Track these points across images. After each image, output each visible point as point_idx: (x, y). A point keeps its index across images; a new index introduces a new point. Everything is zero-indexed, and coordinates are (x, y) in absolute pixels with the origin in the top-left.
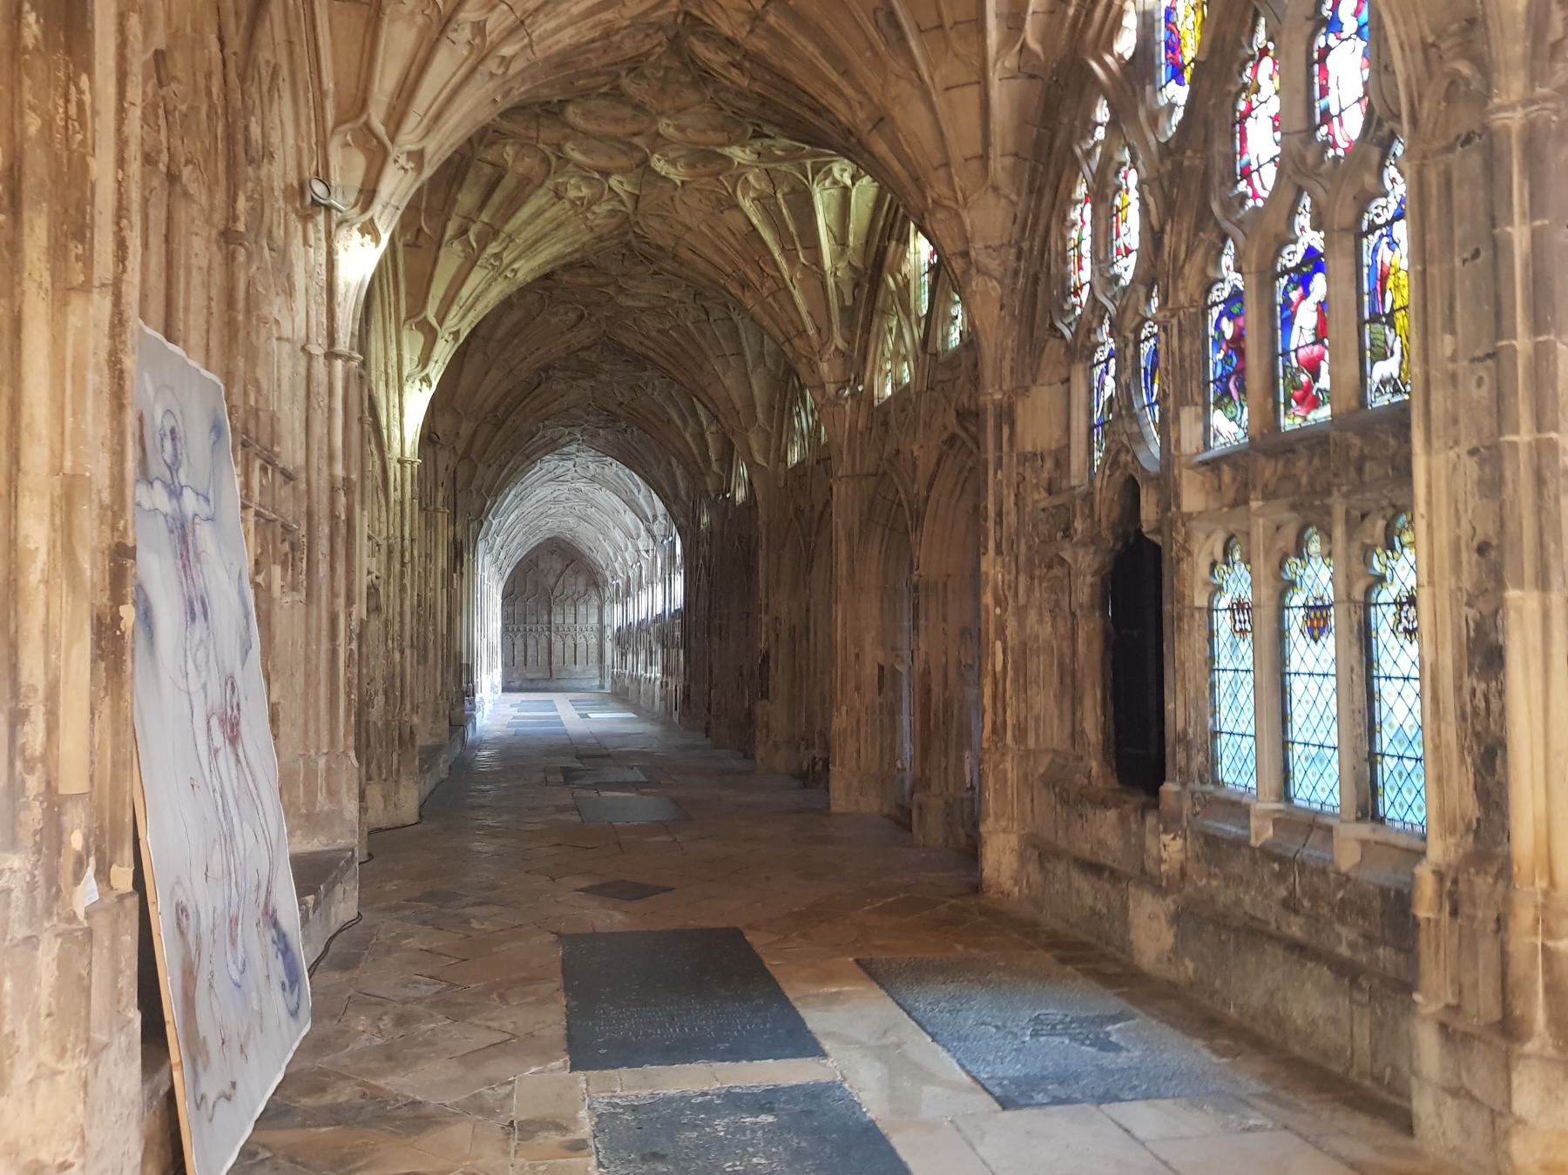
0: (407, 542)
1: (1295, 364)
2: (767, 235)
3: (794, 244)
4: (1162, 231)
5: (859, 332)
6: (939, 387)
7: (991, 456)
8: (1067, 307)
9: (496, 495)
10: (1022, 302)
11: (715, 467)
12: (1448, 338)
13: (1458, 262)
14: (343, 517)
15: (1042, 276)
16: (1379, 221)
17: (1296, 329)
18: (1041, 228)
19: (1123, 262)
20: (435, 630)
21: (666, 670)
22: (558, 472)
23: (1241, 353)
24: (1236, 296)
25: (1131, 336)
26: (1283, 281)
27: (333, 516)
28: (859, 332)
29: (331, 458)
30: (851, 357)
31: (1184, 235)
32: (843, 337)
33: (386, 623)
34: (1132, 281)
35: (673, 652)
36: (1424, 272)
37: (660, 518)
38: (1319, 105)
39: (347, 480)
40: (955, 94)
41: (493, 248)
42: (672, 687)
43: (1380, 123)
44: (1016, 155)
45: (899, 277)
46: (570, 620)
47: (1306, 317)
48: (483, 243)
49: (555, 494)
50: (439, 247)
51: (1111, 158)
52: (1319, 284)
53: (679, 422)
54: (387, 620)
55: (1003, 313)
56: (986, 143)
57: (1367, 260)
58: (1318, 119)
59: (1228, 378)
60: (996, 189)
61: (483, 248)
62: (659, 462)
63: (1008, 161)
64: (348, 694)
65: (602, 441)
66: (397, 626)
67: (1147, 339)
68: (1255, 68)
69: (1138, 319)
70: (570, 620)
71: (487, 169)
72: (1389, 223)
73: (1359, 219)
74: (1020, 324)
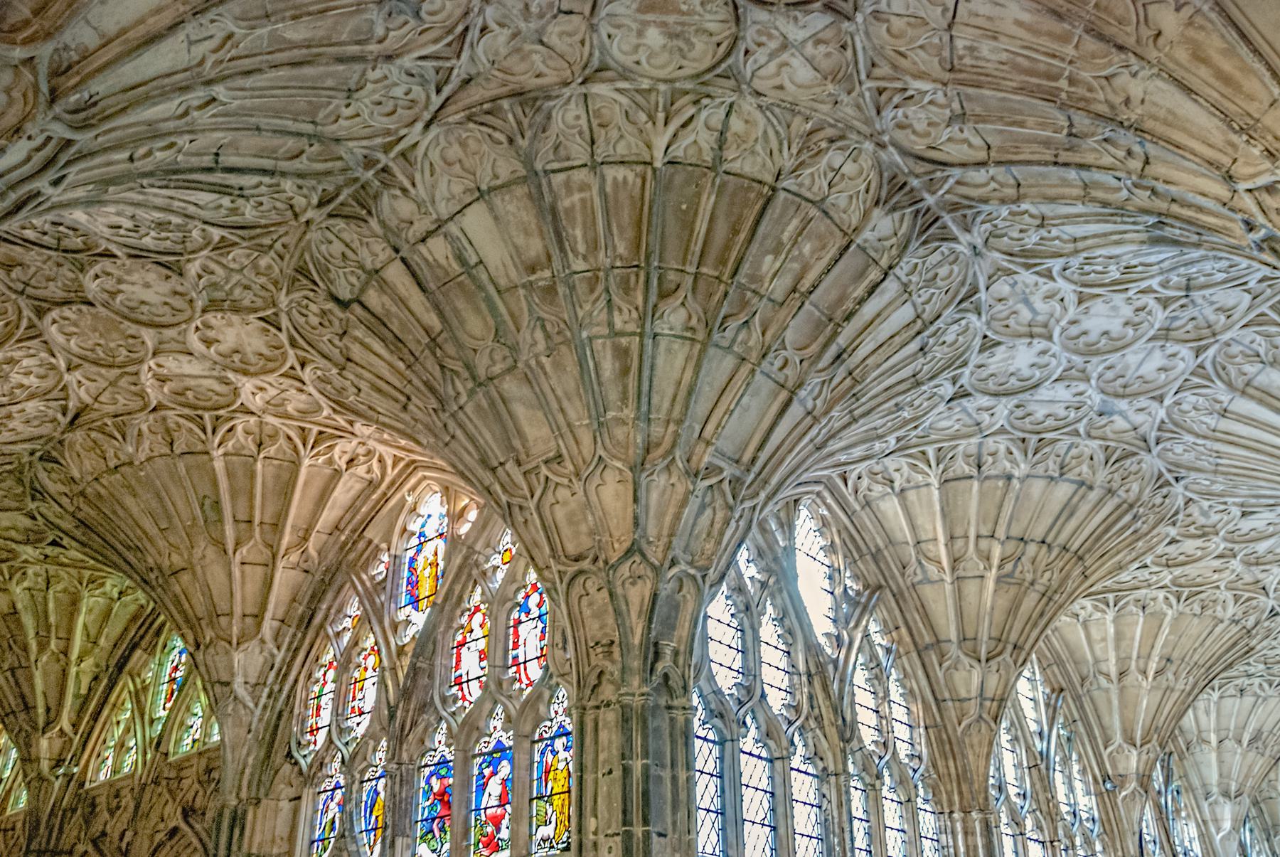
1: (483, 818)
2: (28, 621)
3: (49, 632)
4: (397, 706)
5: (86, 719)
6: (164, 783)
8: (303, 742)
10: (266, 730)
12: (593, 820)
13: (600, 775)
15: (286, 714)
16: (545, 736)
17: (486, 794)
18: (291, 678)
19: (358, 719)
23: (448, 805)
24: (443, 762)
25: (358, 776)
26: (479, 760)
28: (86, 719)
30: (71, 740)
31: (411, 713)
32: (70, 719)
34: (363, 736)
36: (581, 777)
38: (512, 653)
40: (246, 567)
43: (551, 676)
45: (138, 681)
47: (494, 787)
51: (356, 644)
52: (505, 769)
55: (250, 736)
56: (263, 606)
57: (537, 758)
58: (510, 662)
59: (433, 820)
60: (263, 641)
63: (276, 624)
67: (369, 780)
68: (471, 617)
69: (365, 764)
72: (552, 739)
73: (533, 732)
74: (261, 746)
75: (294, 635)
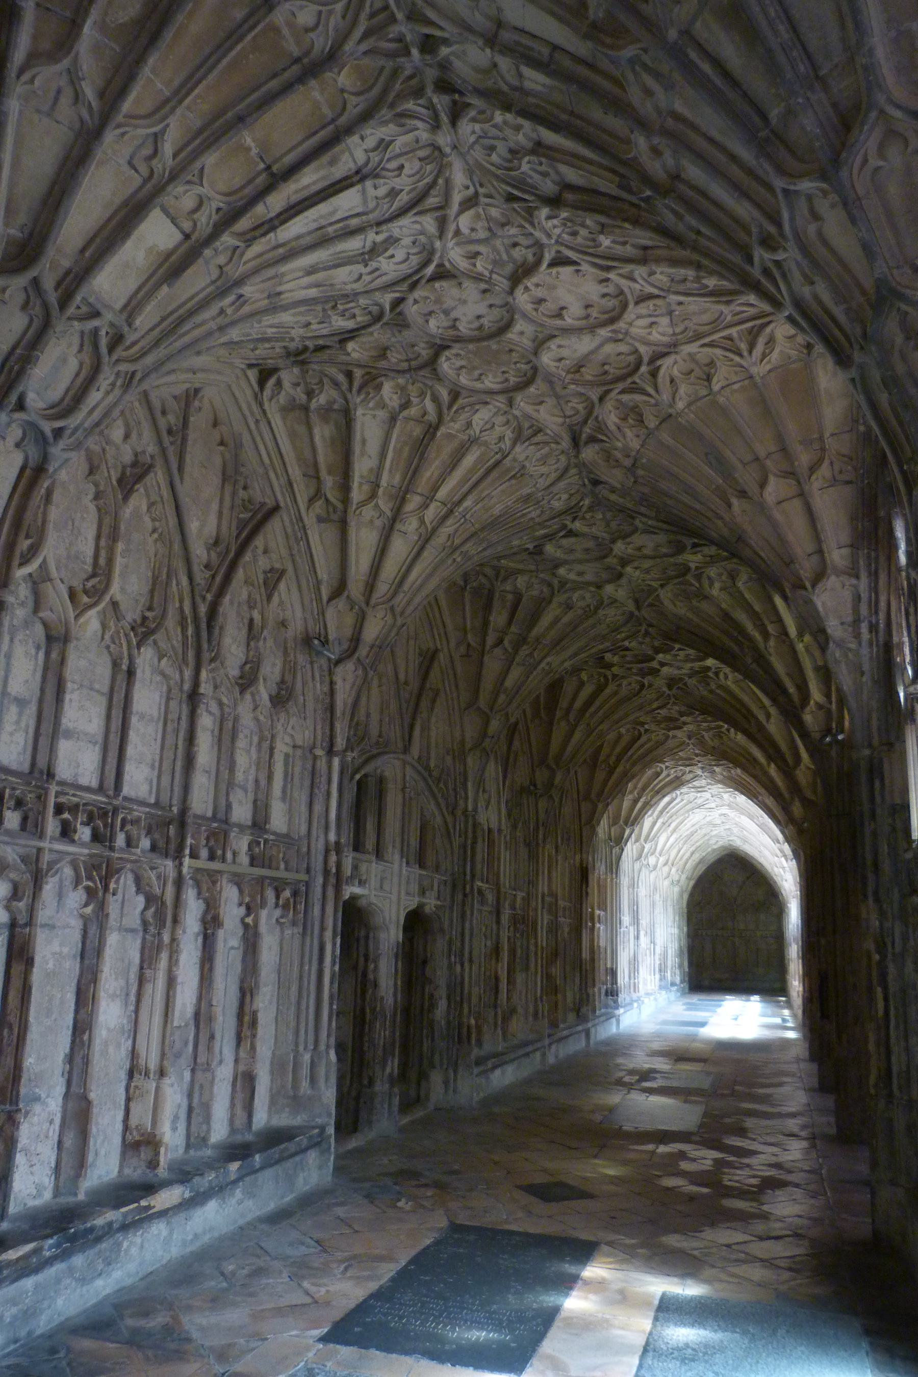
0: (468, 877)
2: (741, 616)
7: (866, 807)
9: (633, 825)
14: (334, 870)
20: (536, 943)
22: (699, 801)
27: (326, 872)
29: (327, 828)
33: (450, 943)
39: (337, 843)
41: (524, 651)
44: (852, 546)
48: (517, 647)
50: (483, 655)
54: (451, 939)
61: (516, 652)
64: (331, 1004)
65: (720, 777)
66: (459, 944)
71: (510, 597)
75: (869, 557)
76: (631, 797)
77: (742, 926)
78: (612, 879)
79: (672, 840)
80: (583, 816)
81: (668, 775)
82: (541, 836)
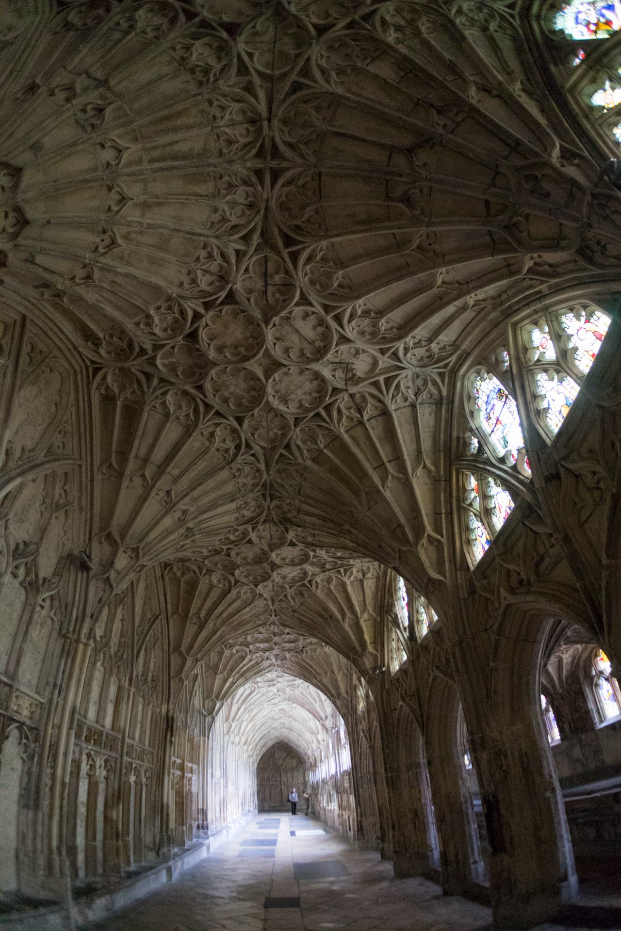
9: (222, 699)
11: (370, 648)
21: (341, 807)
35: (345, 796)
37: (329, 717)
42: (346, 817)
46: (290, 779)
49: (273, 713)
53: (338, 616)
62: (326, 673)
70: (290, 779)
76: (221, 676)
77: (285, 779)
78: (204, 741)
79: (250, 726)
80: (172, 668)
81: (251, 660)
82: (85, 630)
